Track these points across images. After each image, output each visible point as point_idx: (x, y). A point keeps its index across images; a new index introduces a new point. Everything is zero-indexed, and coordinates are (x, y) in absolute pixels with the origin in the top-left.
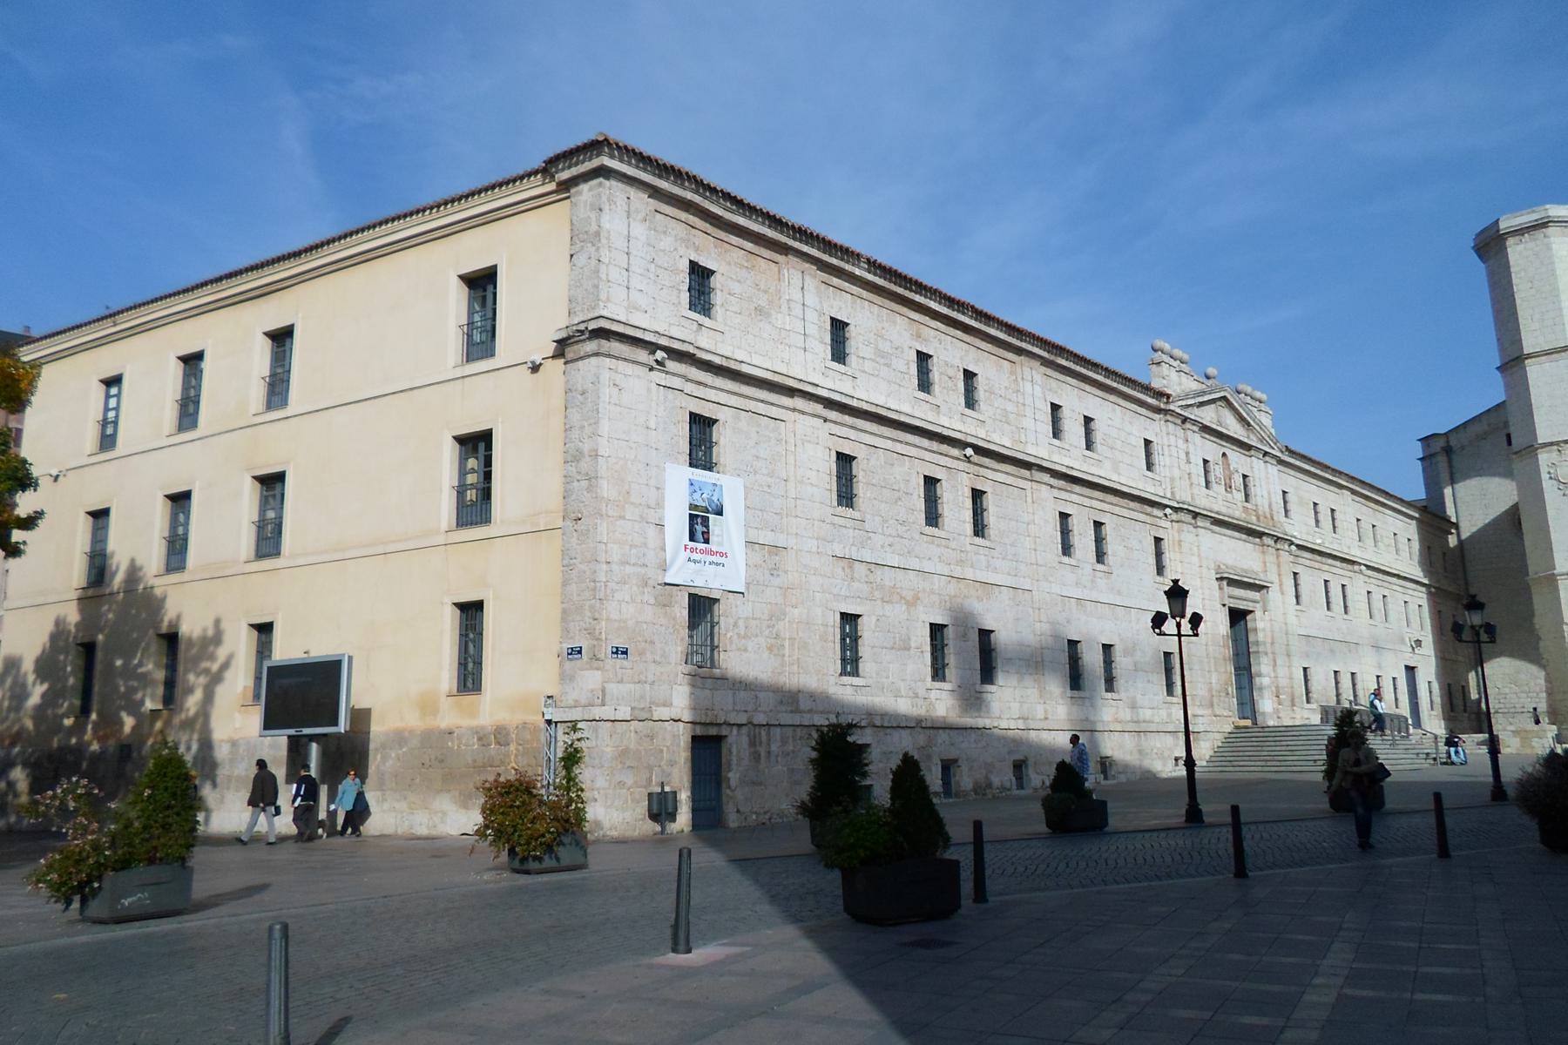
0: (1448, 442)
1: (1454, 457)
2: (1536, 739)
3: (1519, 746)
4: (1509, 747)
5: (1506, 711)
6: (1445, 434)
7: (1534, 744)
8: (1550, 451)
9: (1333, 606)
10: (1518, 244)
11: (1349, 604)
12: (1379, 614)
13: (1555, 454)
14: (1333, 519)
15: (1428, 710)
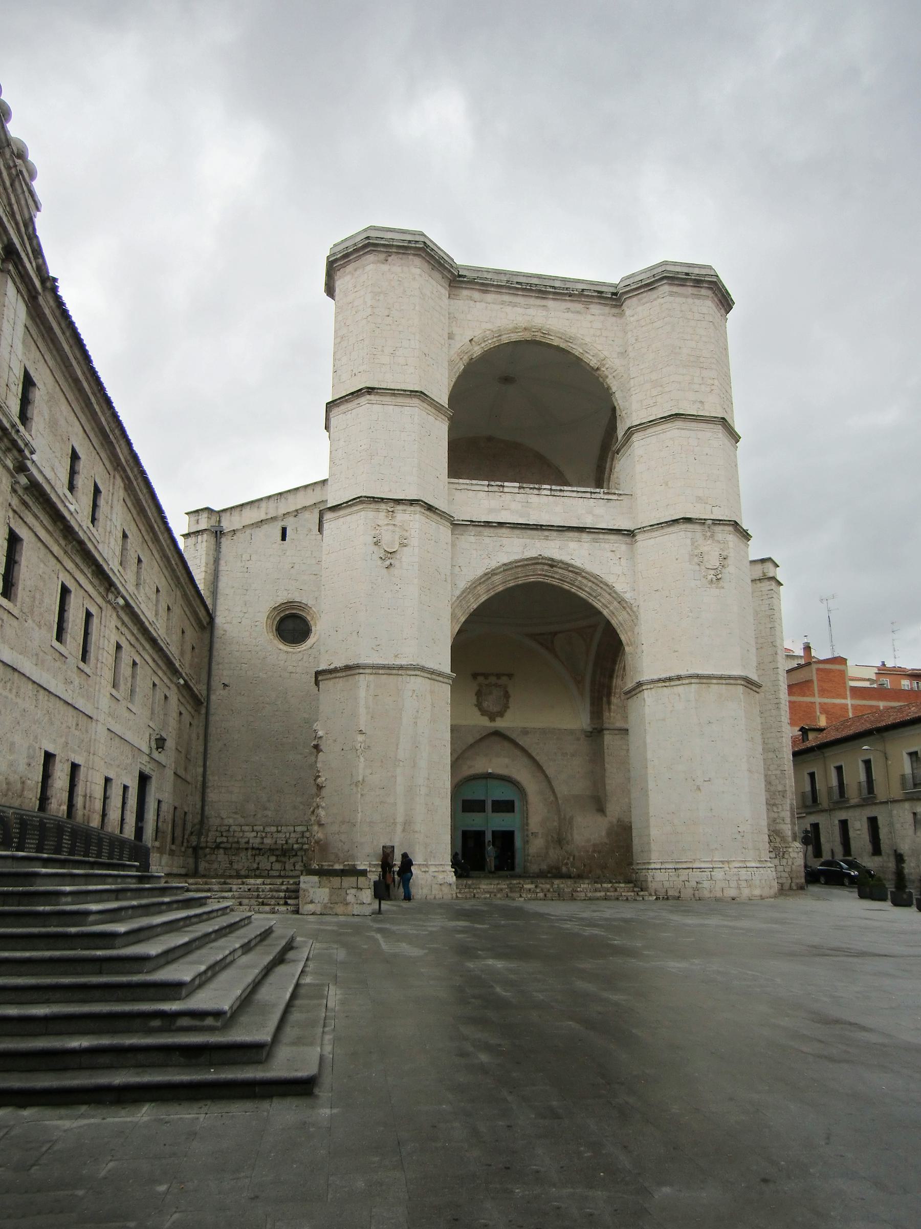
0: (220, 521)
1: (225, 541)
2: (353, 891)
3: (326, 900)
4: (312, 902)
5: (229, 846)
6: (219, 512)
7: (350, 898)
8: (378, 510)
9: (68, 638)
10: (383, 263)
11: (92, 649)
12: (124, 687)
13: (382, 515)
14: (95, 506)
15: (152, 840)
